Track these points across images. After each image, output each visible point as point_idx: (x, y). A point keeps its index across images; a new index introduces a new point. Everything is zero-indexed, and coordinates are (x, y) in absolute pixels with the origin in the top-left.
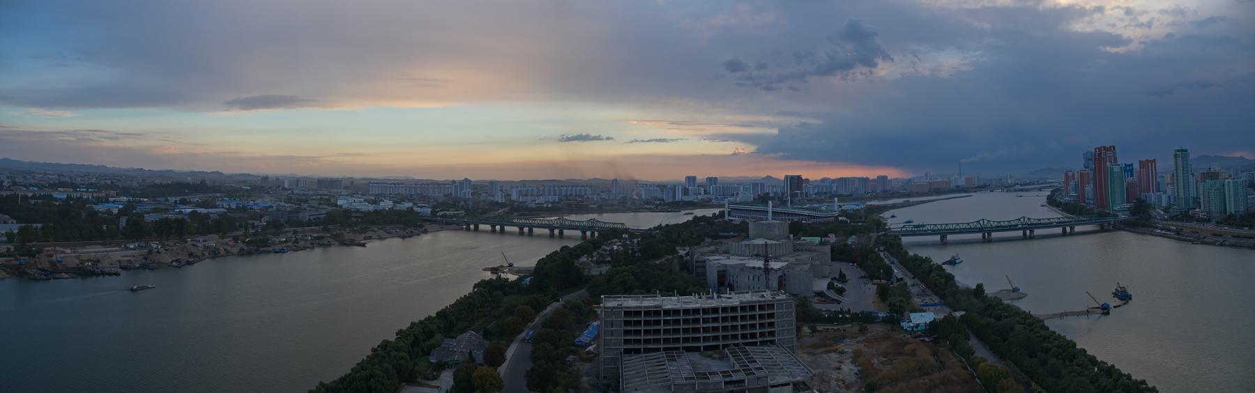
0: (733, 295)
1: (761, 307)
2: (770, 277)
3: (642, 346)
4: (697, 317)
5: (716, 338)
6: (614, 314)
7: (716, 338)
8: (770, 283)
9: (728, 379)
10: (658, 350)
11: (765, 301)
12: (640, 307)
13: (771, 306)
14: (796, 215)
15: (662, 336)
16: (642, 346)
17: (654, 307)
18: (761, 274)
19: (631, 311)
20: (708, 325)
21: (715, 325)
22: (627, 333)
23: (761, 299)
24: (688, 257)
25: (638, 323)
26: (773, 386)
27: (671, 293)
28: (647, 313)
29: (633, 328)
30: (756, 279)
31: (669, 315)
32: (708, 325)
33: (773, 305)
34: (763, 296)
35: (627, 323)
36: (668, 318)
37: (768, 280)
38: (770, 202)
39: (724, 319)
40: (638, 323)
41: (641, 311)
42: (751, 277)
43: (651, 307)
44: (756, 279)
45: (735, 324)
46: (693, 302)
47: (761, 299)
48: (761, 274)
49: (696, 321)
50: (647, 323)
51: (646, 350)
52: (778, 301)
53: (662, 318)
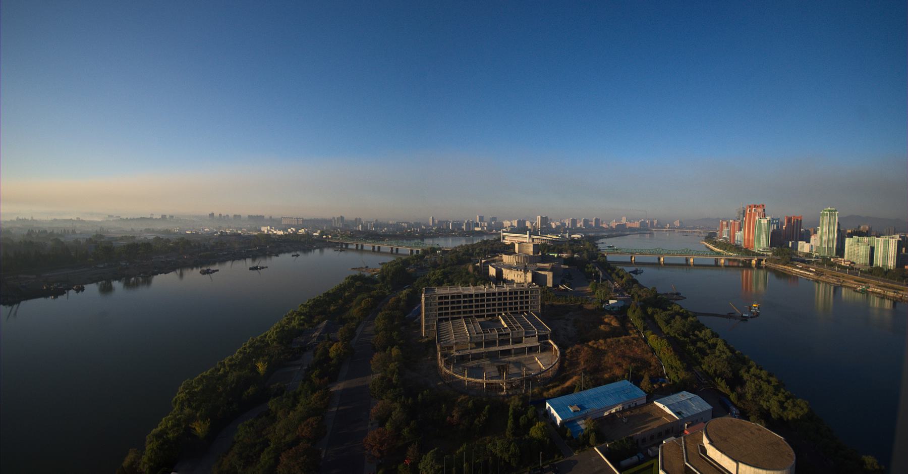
0: (505, 285)
1: (522, 293)
2: (527, 275)
3: (450, 316)
4: (483, 298)
5: (494, 310)
6: (432, 298)
7: (494, 310)
8: (527, 279)
9: (501, 333)
10: (460, 318)
11: (523, 289)
12: (448, 294)
13: (527, 292)
14: (543, 239)
15: (462, 310)
16: (450, 316)
17: (457, 293)
18: (522, 274)
19: (443, 296)
20: (489, 303)
21: (494, 302)
22: (440, 309)
23: (522, 288)
24: (479, 264)
25: (447, 303)
26: (526, 337)
27: (467, 285)
28: (453, 297)
29: (444, 306)
30: (519, 276)
31: (467, 298)
32: (489, 303)
33: (528, 291)
34: (523, 286)
35: (440, 303)
36: (466, 299)
37: (526, 277)
38: (528, 232)
39: (500, 299)
40: (447, 303)
41: (449, 296)
42: (516, 275)
43: (454, 293)
44: (519, 276)
45: (505, 302)
46: (484, 289)
47: (522, 288)
48: (522, 274)
49: (483, 300)
50: (453, 303)
51: (453, 319)
52: (531, 289)
53: (462, 299)
